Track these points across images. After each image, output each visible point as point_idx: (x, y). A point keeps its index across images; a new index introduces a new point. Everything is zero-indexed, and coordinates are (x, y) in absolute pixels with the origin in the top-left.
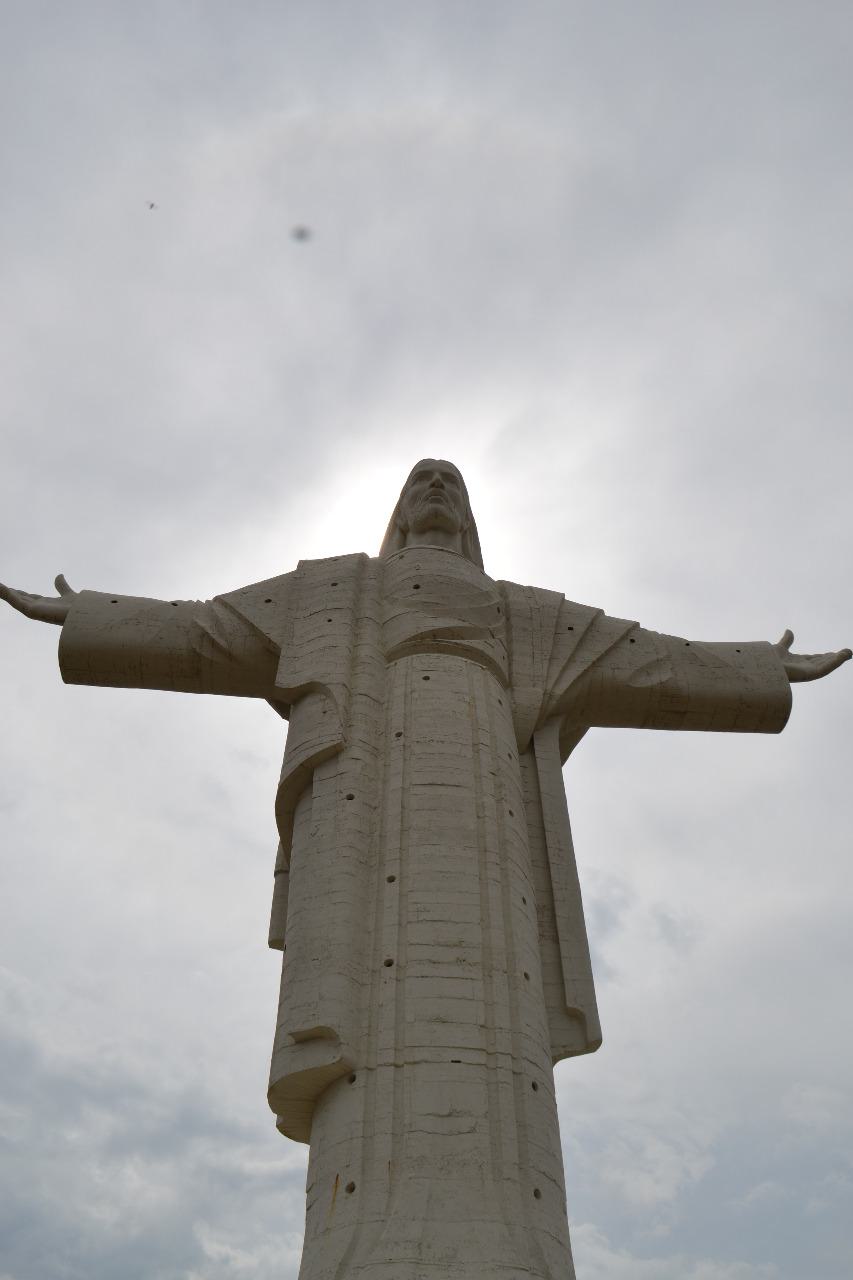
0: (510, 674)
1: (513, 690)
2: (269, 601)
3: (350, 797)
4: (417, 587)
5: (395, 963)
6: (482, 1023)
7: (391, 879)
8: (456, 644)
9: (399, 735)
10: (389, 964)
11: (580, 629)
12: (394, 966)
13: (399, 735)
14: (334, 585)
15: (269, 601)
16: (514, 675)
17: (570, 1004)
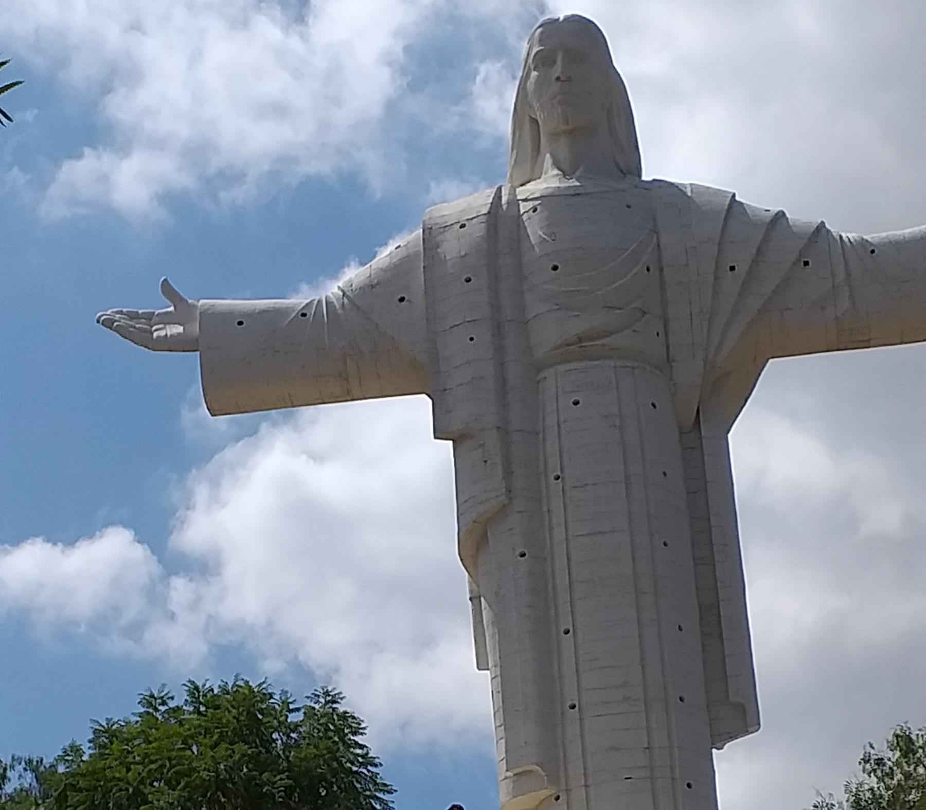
0: (668, 347)
1: (671, 367)
2: (402, 300)
3: (523, 555)
4: (555, 268)
5: (577, 705)
6: (646, 745)
7: (567, 632)
8: (603, 345)
9: (557, 478)
10: (573, 707)
11: (742, 269)
12: (577, 708)
13: (557, 478)
14: (468, 280)
15: (402, 300)
16: (671, 348)
17: (732, 699)
